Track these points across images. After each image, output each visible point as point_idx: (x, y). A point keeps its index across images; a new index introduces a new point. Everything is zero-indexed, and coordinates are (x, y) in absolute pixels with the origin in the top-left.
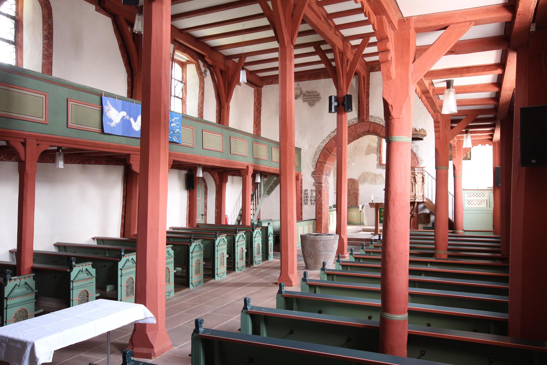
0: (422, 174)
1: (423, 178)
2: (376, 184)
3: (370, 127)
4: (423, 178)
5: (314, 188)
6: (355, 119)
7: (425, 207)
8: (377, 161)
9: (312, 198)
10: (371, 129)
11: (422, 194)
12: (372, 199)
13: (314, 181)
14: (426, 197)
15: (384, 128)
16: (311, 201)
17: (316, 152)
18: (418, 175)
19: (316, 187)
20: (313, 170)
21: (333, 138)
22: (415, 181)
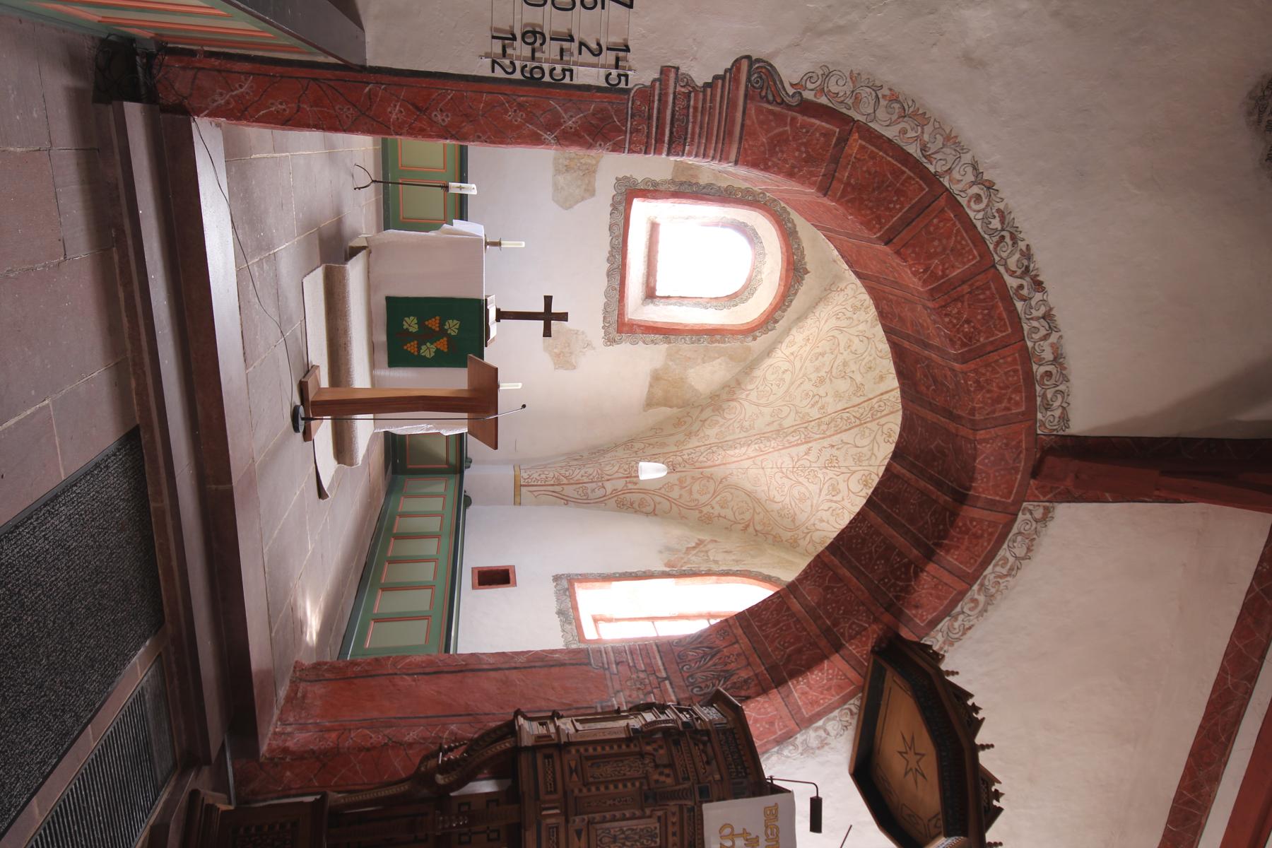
2: (558, 171)
3: (991, 505)
5: (642, 75)
6: (1064, 418)
8: (646, 181)
9: (552, 49)
12: (505, 244)
13: (701, 76)
16: (533, 35)
17: (920, 117)
19: (645, 93)
20: (791, 71)
21: (987, 265)
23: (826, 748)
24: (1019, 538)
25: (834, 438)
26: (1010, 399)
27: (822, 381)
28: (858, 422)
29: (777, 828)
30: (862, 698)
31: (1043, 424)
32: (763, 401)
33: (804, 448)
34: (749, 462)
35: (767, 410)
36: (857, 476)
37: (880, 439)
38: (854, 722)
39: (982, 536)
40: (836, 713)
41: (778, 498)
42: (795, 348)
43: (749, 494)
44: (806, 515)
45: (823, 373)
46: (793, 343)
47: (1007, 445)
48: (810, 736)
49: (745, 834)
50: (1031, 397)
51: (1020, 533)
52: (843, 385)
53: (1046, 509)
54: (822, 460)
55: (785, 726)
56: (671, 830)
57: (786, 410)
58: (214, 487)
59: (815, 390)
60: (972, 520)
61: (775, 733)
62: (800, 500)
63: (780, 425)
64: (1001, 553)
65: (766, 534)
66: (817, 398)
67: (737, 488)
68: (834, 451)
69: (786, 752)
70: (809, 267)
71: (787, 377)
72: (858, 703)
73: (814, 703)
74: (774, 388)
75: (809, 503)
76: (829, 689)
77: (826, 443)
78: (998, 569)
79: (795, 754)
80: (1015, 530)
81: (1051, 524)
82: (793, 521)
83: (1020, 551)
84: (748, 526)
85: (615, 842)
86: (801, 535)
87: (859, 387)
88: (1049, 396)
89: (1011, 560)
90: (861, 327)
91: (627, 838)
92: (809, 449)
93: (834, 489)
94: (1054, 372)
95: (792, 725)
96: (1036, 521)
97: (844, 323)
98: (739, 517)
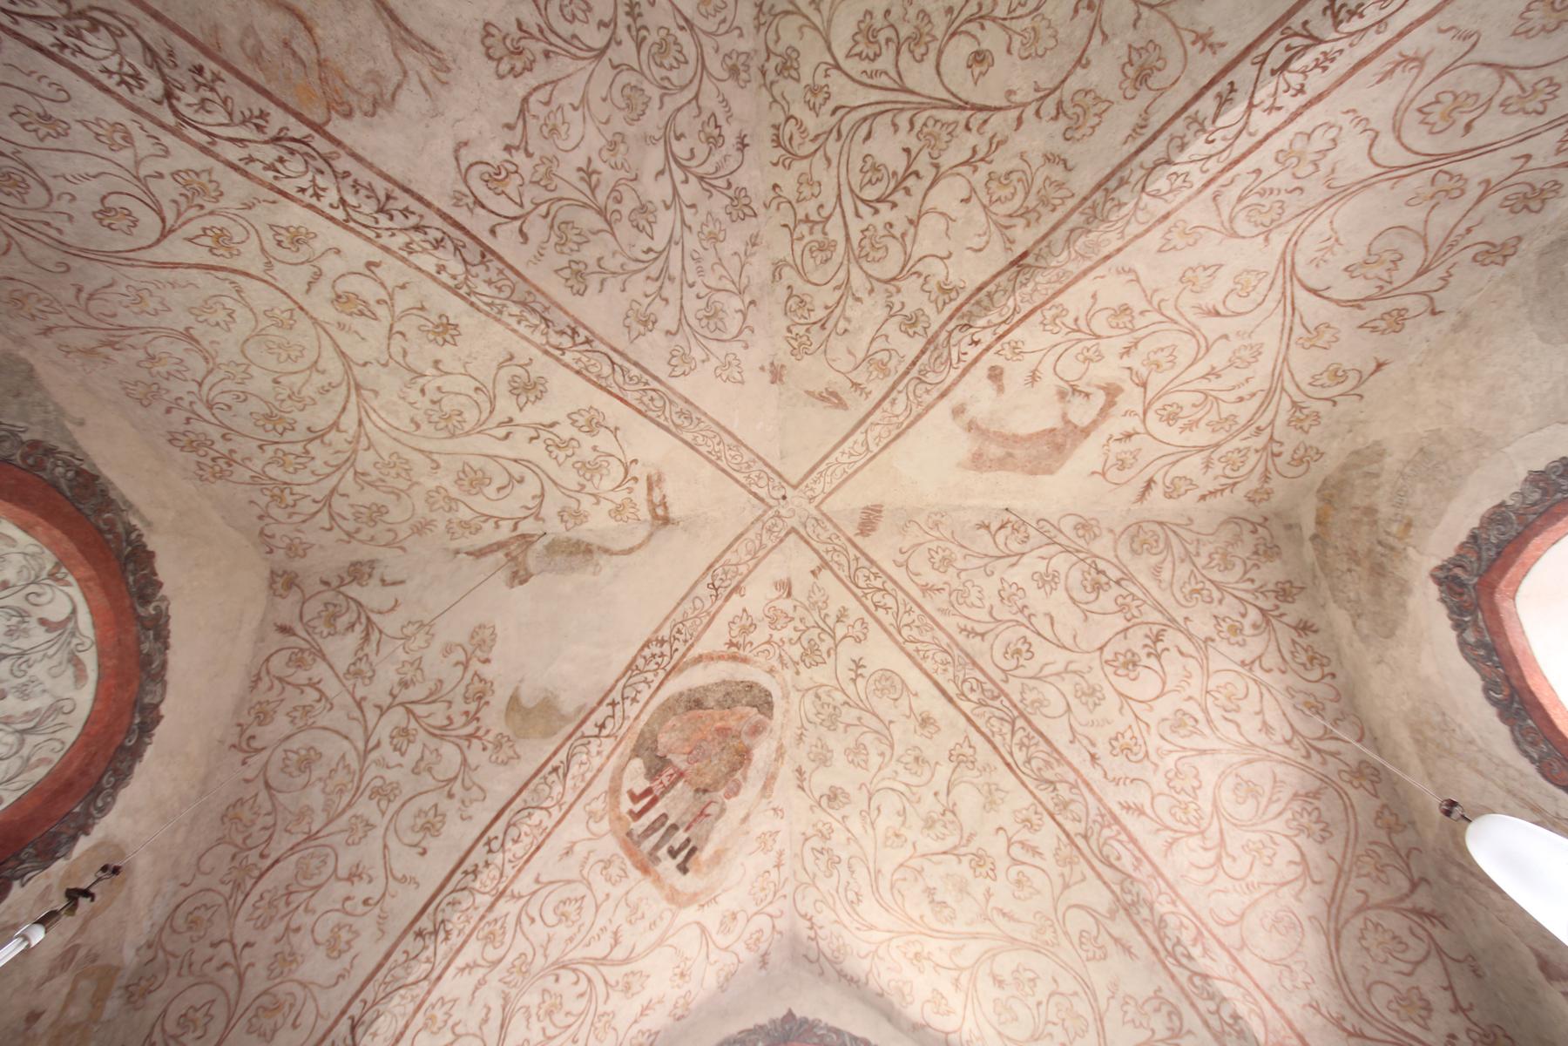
25: (1075, 761)
27: (979, 859)
28: (1020, 723)
32: (1083, 1007)
33: (1127, 819)
34: (1246, 958)
35: (1099, 977)
36: (1124, 685)
37: (1031, 668)
41: (1287, 852)
42: (946, 988)
43: (1335, 938)
44: (1280, 770)
45: (964, 869)
46: (938, 997)
52: (968, 800)
54: (1134, 771)
57: (1078, 922)
59: (1003, 864)
62: (1254, 793)
63: (1112, 915)
65: (1405, 857)
66: (1016, 851)
67: (1340, 980)
68: (1102, 750)
70: (780, 1013)
71: (1006, 964)
74: (1042, 990)
75: (1246, 772)
77: (1093, 775)
82: (1316, 795)
84: (1420, 912)
86: (1333, 766)
87: (959, 760)
90: (856, 825)
92: (1128, 808)
93: (1182, 725)
97: (862, 875)
98: (1417, 949)
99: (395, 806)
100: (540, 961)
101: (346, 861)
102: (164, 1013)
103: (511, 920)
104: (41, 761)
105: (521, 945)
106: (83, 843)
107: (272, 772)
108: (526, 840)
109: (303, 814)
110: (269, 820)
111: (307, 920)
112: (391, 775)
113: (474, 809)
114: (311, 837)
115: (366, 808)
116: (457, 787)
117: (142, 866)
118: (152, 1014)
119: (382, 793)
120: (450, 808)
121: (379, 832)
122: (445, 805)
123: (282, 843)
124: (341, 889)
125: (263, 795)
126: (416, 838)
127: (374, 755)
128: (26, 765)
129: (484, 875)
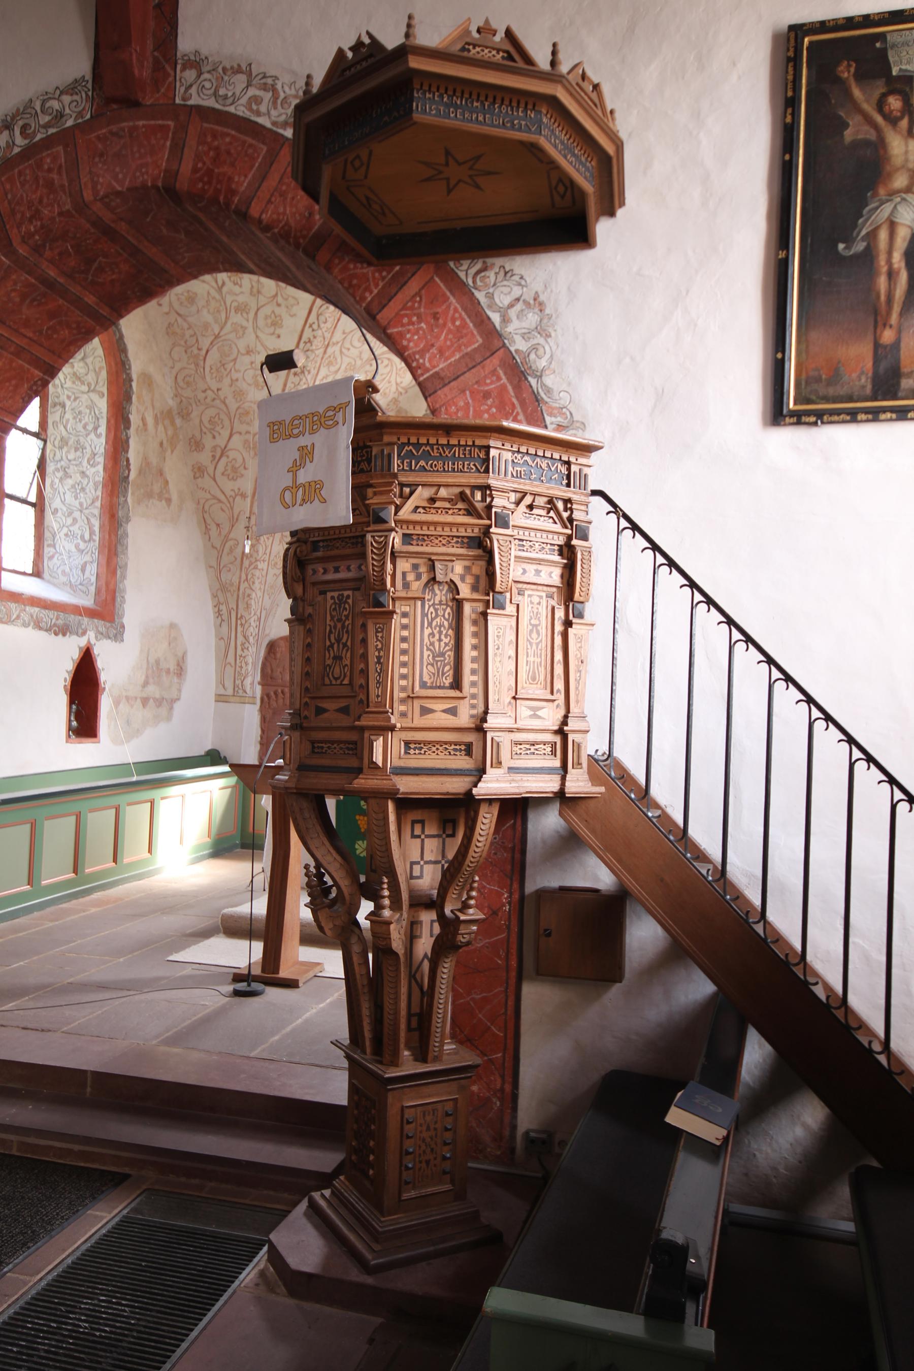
0: (563, 511)
1: (568, 551)
3: (177, 149)
4: (568, 551)
6: (72, 88)
7: (570, 842)
10: (186, 168)
11: (551, 716)
14: (593, 744)
15: (285, 157)
18: (519, 517)
22: (487, 581)
23: (542, 298)
24: (222, 92)
26: (50, 170)
29: (294, 419)
30: (457, 260)
31: (80, 114)
38: (498, 261)
39: (217, 149)
40: (480, 296)
47: (101, 155)
48: (517, 333)
49: (295, 468)
50: (49, 142)
51: (215, 94)
53: (184, 69)
55: (494, 372)
56: (330, 576)
58: (89, 1090)
60: (195, 170)
61: (503, 388)
64: (240, 110)
69: (542, 363)
72: (465, 264)
73: (460, 333)
76: (435, 316)
78: (263, 108)
79: (549, 347)
80: (211, 103)
81: (204, 52)
83: (241, 79)
85: (340, 658)
88: (47, 118)
89: (252, 92)
91: (338, 640)
94: (21, 123)
95: (495, 361)
96: (200, 74)
99: (252, 315)
100: (359, 363)
101: (242, 345)
102: (201, 421)
103: (337, 353)
104: (101, 368)
105: (346, 360)
106: (134, 384)
107: (176, 306)
108: (330, 320)
109: (206, 326)
110: (191, 332)
111: (240, 375)
112: (241, 299)
113: (294, 310)
114: (217, 337)
115: (236, 318)
116: (280, 299)
117: (151, 370)
118: (197, 421)
119: (241, 309)
120: (281, 311)
121: (250, 329)
122: (278, 311)
123: (205, 343)
124: (247, 359)
125: (180, 320)
126: (271, 330)
127: (225, 290)
128: (97, 374)
129: (315, 342)
